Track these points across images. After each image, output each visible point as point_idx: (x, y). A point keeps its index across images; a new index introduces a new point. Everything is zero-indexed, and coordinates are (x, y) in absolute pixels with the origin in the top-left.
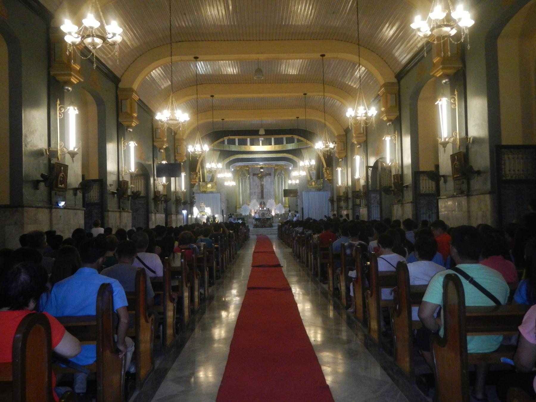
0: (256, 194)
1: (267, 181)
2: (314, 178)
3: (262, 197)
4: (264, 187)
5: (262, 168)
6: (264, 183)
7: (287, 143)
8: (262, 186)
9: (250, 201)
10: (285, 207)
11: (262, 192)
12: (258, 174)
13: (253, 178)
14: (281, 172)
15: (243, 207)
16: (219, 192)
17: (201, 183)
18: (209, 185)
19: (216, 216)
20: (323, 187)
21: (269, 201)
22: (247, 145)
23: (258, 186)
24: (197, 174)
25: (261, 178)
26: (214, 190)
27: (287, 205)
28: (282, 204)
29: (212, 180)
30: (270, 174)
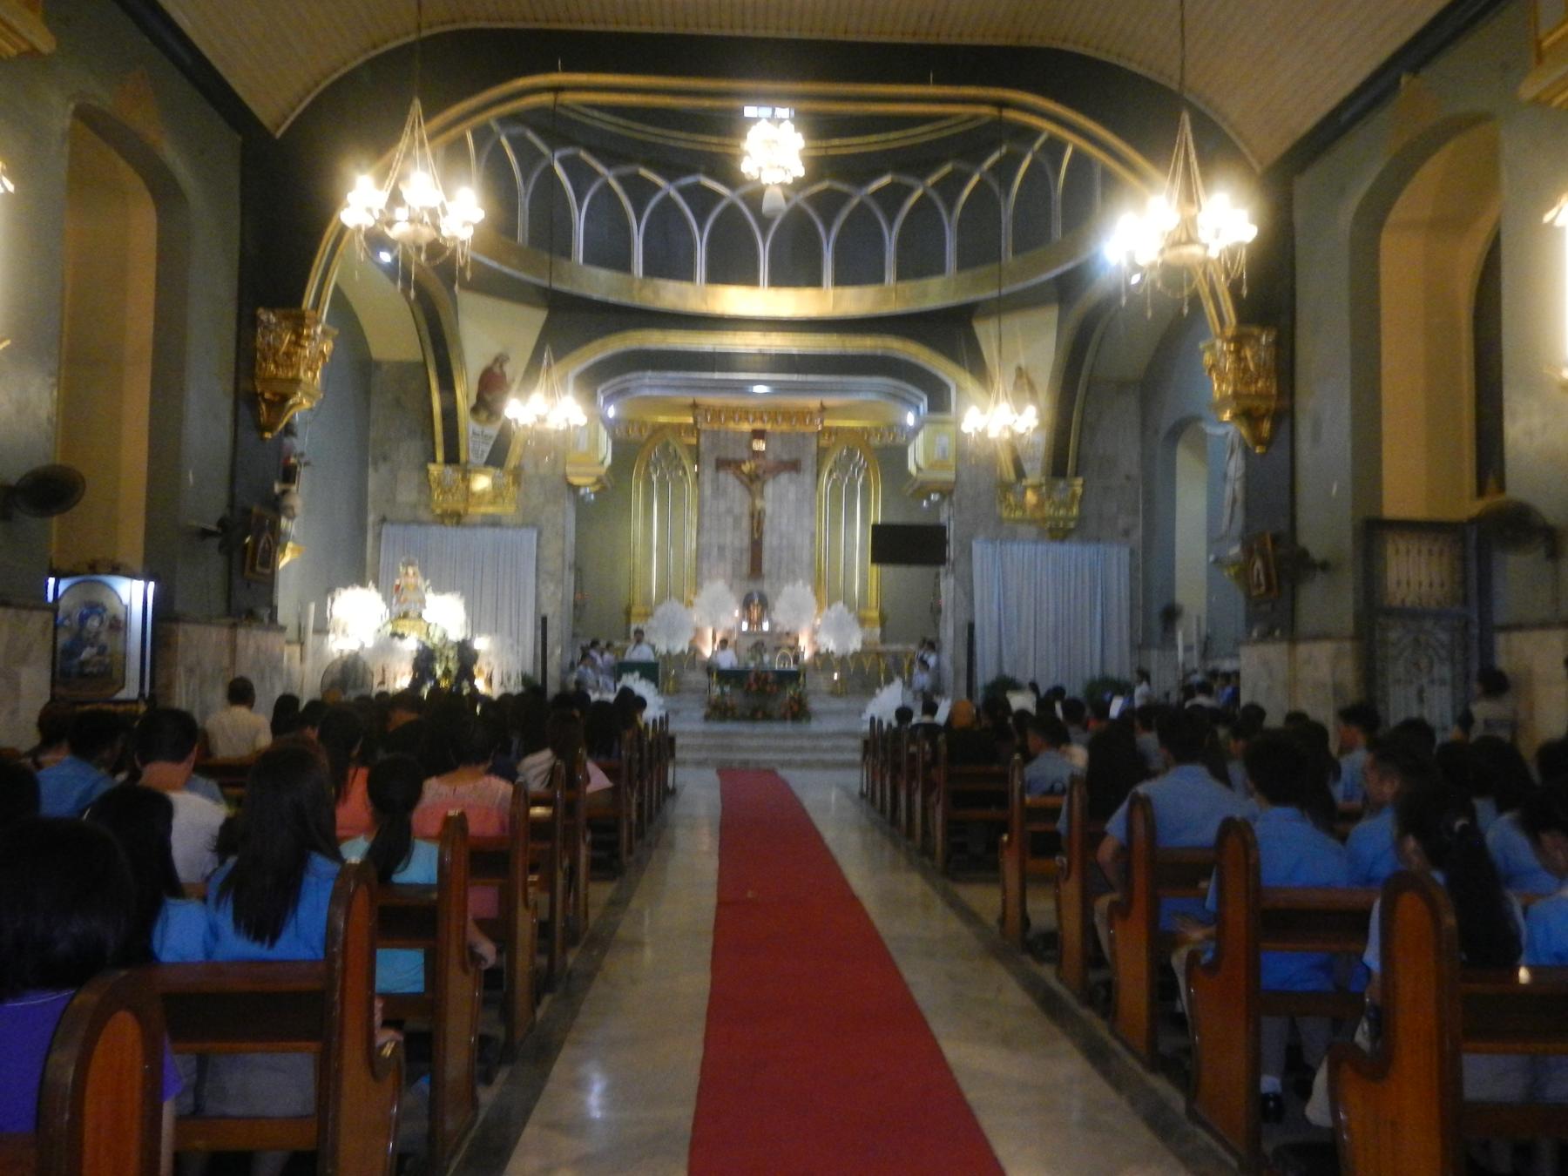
0: (728, 554)
1: (779, 496)
2: (1035, 473)
3: (756, 569)
4: (767, 526)
5: (759, 434)
6: (767, 504)
7: (901, 276)
8: (757, 519)
9: (698, 585)
10: (862, 621)
11: (756, 547)
13: (715, 481)
14: (851, 454)
15: (660, 611)
16: (525, 525)
17: (434, 469)
18: (481, 483)
19: (481, 644)
20: (1081, 520)
21: (787, 589)
22: (687, 275)
23: (737, 520)
24: (299, 324)
25: (753, 482)
26: (507, 509)
27: (875, 614)
28: (848, 602)
29: (497, 457)
30: (794, 466)
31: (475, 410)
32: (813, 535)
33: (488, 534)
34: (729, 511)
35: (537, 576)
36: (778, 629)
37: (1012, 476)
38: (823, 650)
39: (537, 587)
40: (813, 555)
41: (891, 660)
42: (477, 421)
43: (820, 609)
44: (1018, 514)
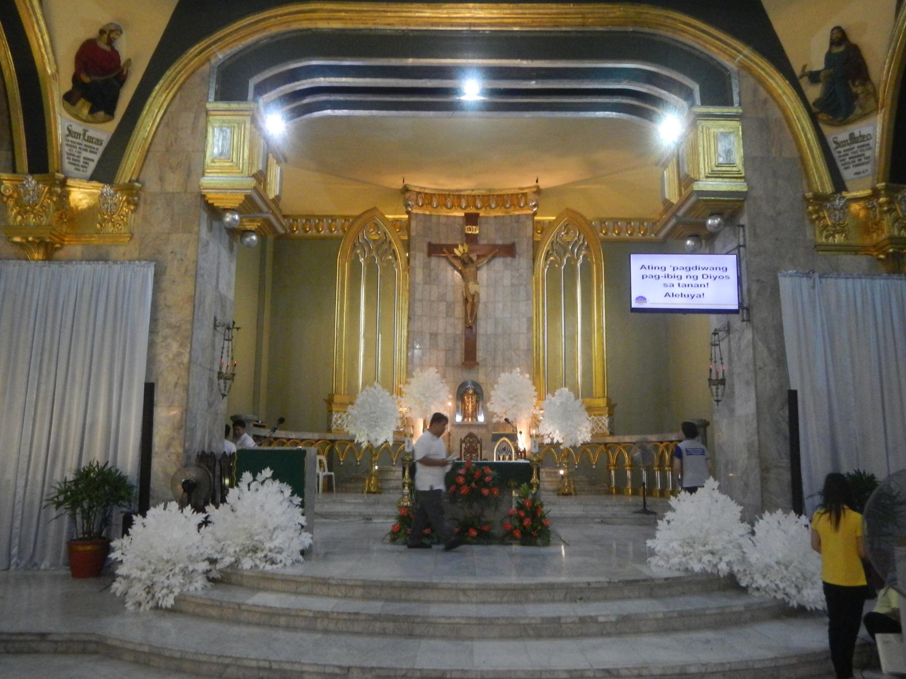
3: (470, 357)
5: (472, 219)
12: (450, 248)
13: (427, 267)
21: (504, 377)
23: (450, 306)
27: (602, 402)
30: (509, 250)
31: (69, 98)
32: (530, 320)
33: (86, 268)
34: (442, 298)
35: (153, 331)
36: (495, 420)
37: (829, 189)
38: (547, 441)
39: (151, 345)
40: (530, 343)
41: (637, 454)
42: (77, 117)
43: (540, 398)
44: (838, 239)
